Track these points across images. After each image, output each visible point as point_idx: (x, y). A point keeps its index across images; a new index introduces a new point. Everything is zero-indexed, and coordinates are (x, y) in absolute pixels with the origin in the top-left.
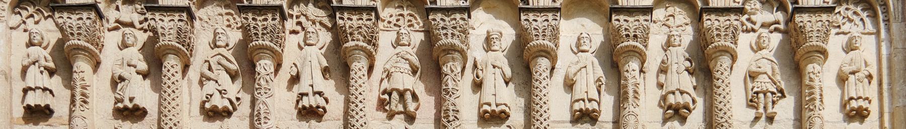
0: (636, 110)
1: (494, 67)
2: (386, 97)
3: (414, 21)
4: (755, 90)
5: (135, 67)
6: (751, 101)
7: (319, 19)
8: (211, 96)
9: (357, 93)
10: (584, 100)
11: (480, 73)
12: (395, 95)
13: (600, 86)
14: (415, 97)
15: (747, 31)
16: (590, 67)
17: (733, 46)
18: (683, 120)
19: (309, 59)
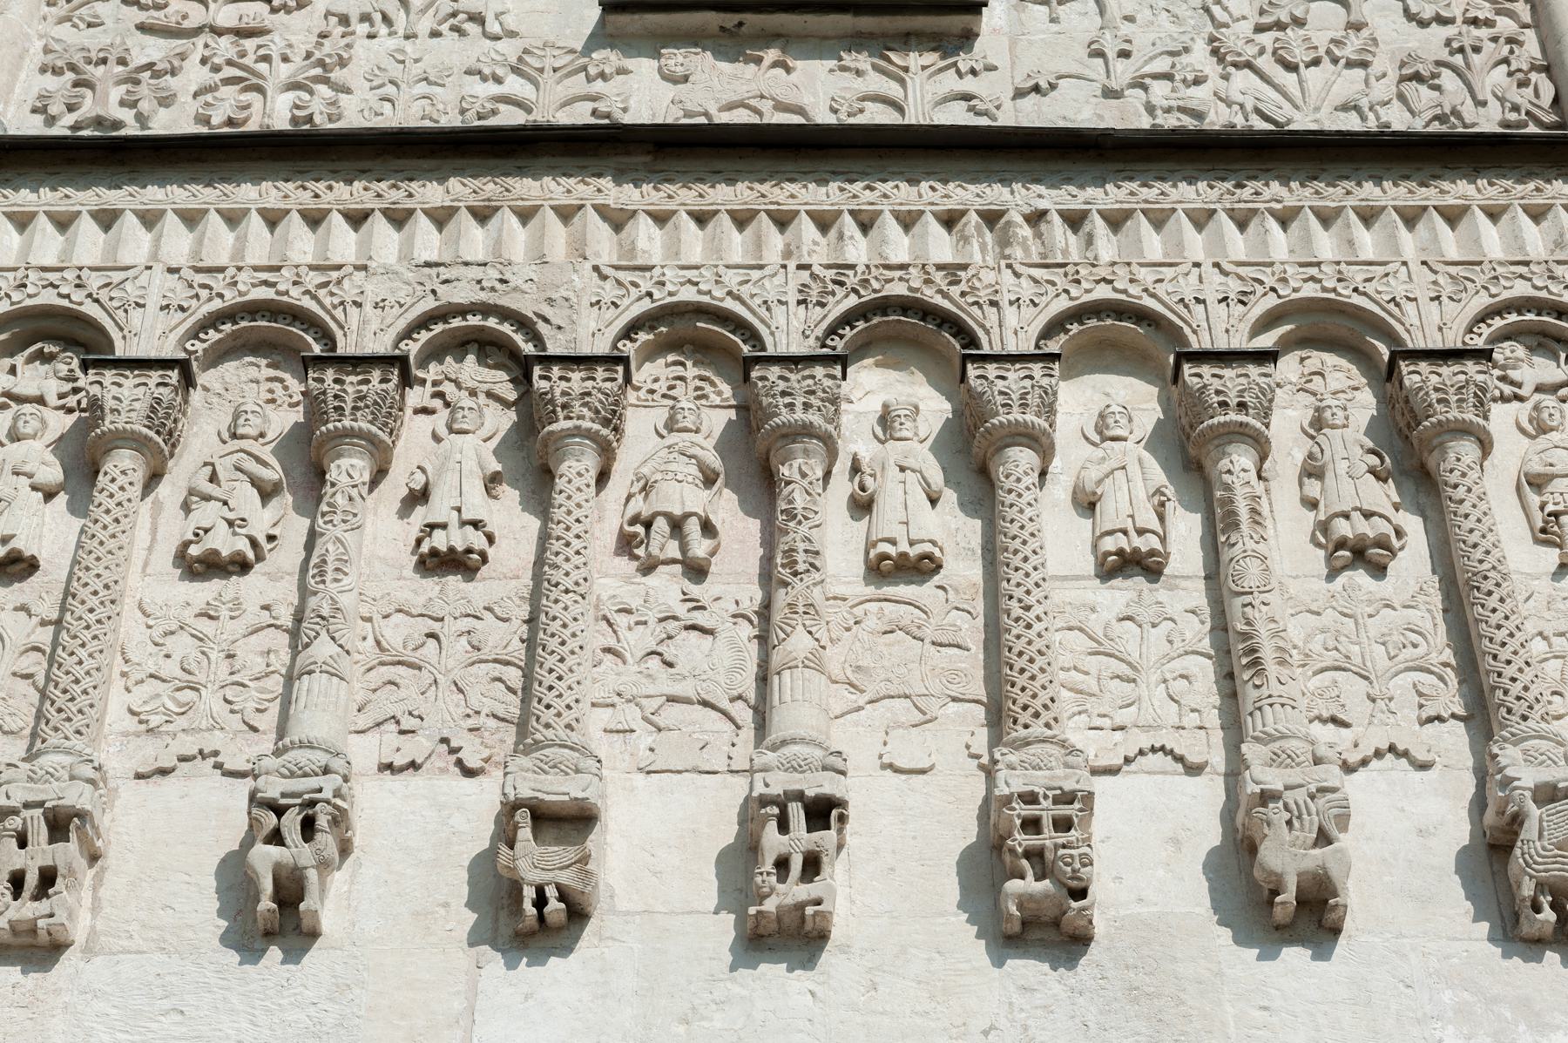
0: (1261, 548)
1: (902, 469)
2: (639, 529)
3: (708, 389)
4: (1550, 508)
5: (30, 476)
6: (1543, 531)
7: (486, 387)
8: (206, 531)
9: (572, 519)
10: (1125, 532)
11: (869, 482)
12: (661, 525)
13: (1162, 504)
14: (708, 528)
15: (1504, 399)
16: (1134, 469)
17: (1481, 421)
18: (1379, 571)
19: (458, 457)
